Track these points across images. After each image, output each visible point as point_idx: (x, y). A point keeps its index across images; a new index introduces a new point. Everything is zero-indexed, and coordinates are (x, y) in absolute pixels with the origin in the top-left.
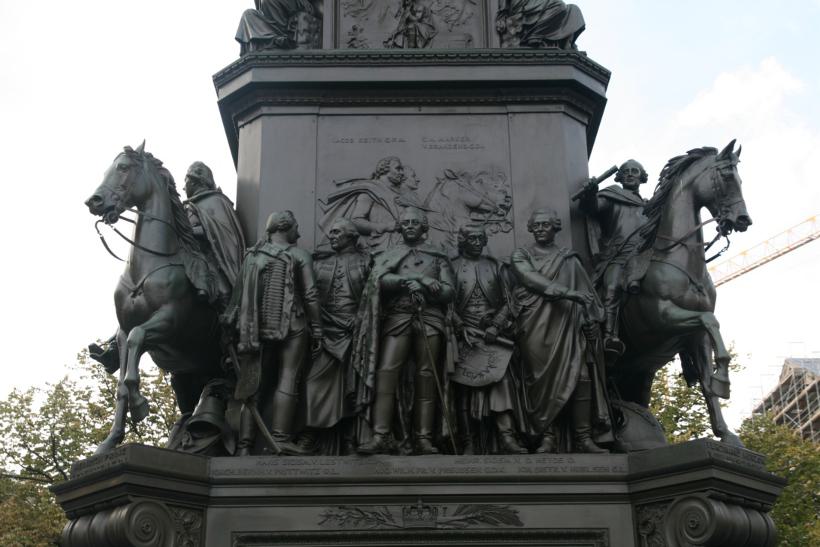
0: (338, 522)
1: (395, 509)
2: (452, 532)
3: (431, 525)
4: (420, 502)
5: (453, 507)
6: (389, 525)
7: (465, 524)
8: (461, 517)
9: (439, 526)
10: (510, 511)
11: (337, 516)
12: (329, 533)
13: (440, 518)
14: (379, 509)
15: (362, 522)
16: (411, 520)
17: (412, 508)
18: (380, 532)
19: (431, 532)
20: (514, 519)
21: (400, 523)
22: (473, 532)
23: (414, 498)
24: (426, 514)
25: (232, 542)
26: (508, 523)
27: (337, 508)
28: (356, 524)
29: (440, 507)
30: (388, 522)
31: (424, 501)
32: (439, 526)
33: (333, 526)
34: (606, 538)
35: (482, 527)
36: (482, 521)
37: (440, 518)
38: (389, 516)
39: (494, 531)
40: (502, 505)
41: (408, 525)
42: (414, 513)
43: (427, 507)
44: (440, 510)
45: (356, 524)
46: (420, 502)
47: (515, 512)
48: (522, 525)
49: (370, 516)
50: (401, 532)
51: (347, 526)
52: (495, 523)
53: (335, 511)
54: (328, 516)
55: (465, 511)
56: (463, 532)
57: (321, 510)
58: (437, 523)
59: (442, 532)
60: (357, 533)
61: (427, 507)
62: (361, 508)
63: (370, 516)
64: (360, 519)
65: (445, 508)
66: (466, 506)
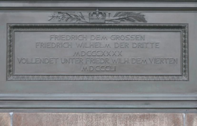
0: (58, 19)
1: (85, 14)
2: (113, 25)
3: (102, 21)
4: (97, 10)
5: (114, 13)
6: (82, 22)
7: (119, 21)
8: (117, 18)
9: (106, 22)
10: (140, 15)
11: (57, 16)
12: (53, 25)
13: (107, 18)
14: (78, 13)
15: (69, 20)
16: (93, 19)
17: (94, 13)
18: (78, 25)
19: (103, 25)
20: (142, 19)
21: (88, 20)
22: (123, 25)
23: (95, 9)
24: (100, 16)
25: (7, 28)
26: (140, 21)
27: (57, 13)
28: (67, 20)
29: (107, 13)
30: (82, 20)
31: (99, 10)
32: (106, 22)
33: (56, 21)
34: (186, 29)
35: (127, 23)
36: (127, 20)
37: (107, 18)
38: (83, 17)
39: (133, 25)
40: (137, 12)
41: (92, 21)
42: (95, 16)
43: (101, 13)
44: (107, 14)
45: (67, 20)
46: (97, 10)
47: (143, 16)
48: (147, 22)
49: (73, 17)
50: (88, 25)
51: (62, 22)
52: (134, 21)
53: (56, 14)
54: (53, 17)
55: (119, 15)
56: (118, 25)
57: (50, 14)
58: (106, 21)
59: (108, 25)
60: (67, 25)
61: (101, 13)
62: (69, 13)
63: (73, 17)
64: (68, 18)
65: (110, 14)
66: (120, 13)
